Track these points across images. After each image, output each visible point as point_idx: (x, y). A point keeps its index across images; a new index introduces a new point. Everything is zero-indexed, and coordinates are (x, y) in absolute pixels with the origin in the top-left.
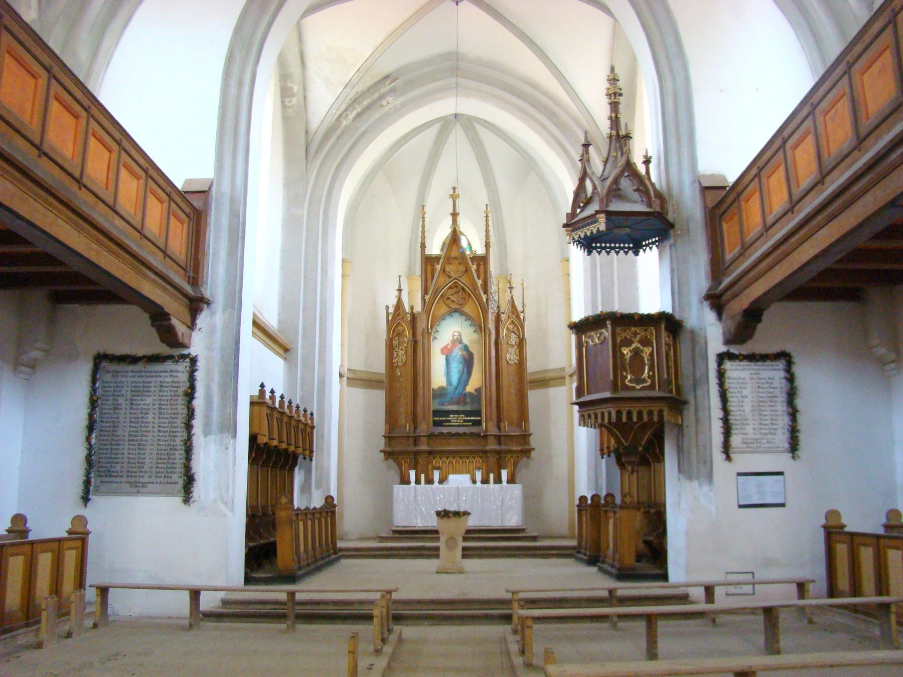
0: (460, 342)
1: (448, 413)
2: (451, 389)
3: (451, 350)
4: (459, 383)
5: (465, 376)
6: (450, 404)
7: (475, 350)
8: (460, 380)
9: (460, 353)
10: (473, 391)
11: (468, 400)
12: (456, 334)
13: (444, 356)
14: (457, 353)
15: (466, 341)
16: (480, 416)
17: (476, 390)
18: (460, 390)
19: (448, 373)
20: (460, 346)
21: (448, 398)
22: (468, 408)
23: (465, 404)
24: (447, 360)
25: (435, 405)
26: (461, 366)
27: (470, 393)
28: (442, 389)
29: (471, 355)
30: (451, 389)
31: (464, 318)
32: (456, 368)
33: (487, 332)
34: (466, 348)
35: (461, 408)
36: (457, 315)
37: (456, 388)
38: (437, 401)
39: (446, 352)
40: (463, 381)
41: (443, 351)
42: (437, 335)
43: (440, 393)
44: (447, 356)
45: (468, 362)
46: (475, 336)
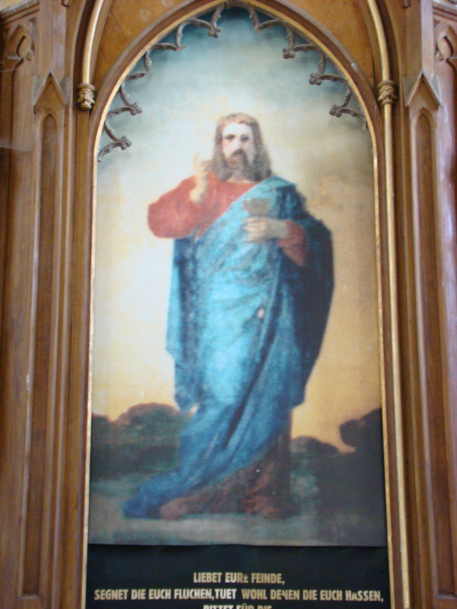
0: (259, 170)
1: (181, 561)
2: (202, 422)
3: (205, 215)
4: (248, 389)
5: (284, 351)
6: (195, 511)
7: (334, 211)
8: (255, 368)
9: (256, 229)
10: (332, 437)
11: (303, 484)
12: (237, 129)
13: (166, 248)
14: (242, 228)
15: (286, 166)
16: (378, 577)
17: (348, 430)
18: (256, 425)
19: (188, 336)
20: (258, 191)
21: (189, 471)
22: (302, 532)
23: (286, 508)
24: (181, 263)
25: (109, 516)
26: (261, 298)
27: (314, 446)
28: (148, 418)
29: (317, 239)
30: (202, 422)
31: (281, 44)
32: (234, 304)
33: (412, 99)
34: (290, 201)
35: (260, 532)
36: (239, 34)
37: (237, 413)
38: (121, 488)
39: (178, 219)
40: (271, 381)
41: (158, 218)
42: (127, 127)
43: (142, 445)
44: (182, 243)
45: (303, 273)
46: (338, 142)
